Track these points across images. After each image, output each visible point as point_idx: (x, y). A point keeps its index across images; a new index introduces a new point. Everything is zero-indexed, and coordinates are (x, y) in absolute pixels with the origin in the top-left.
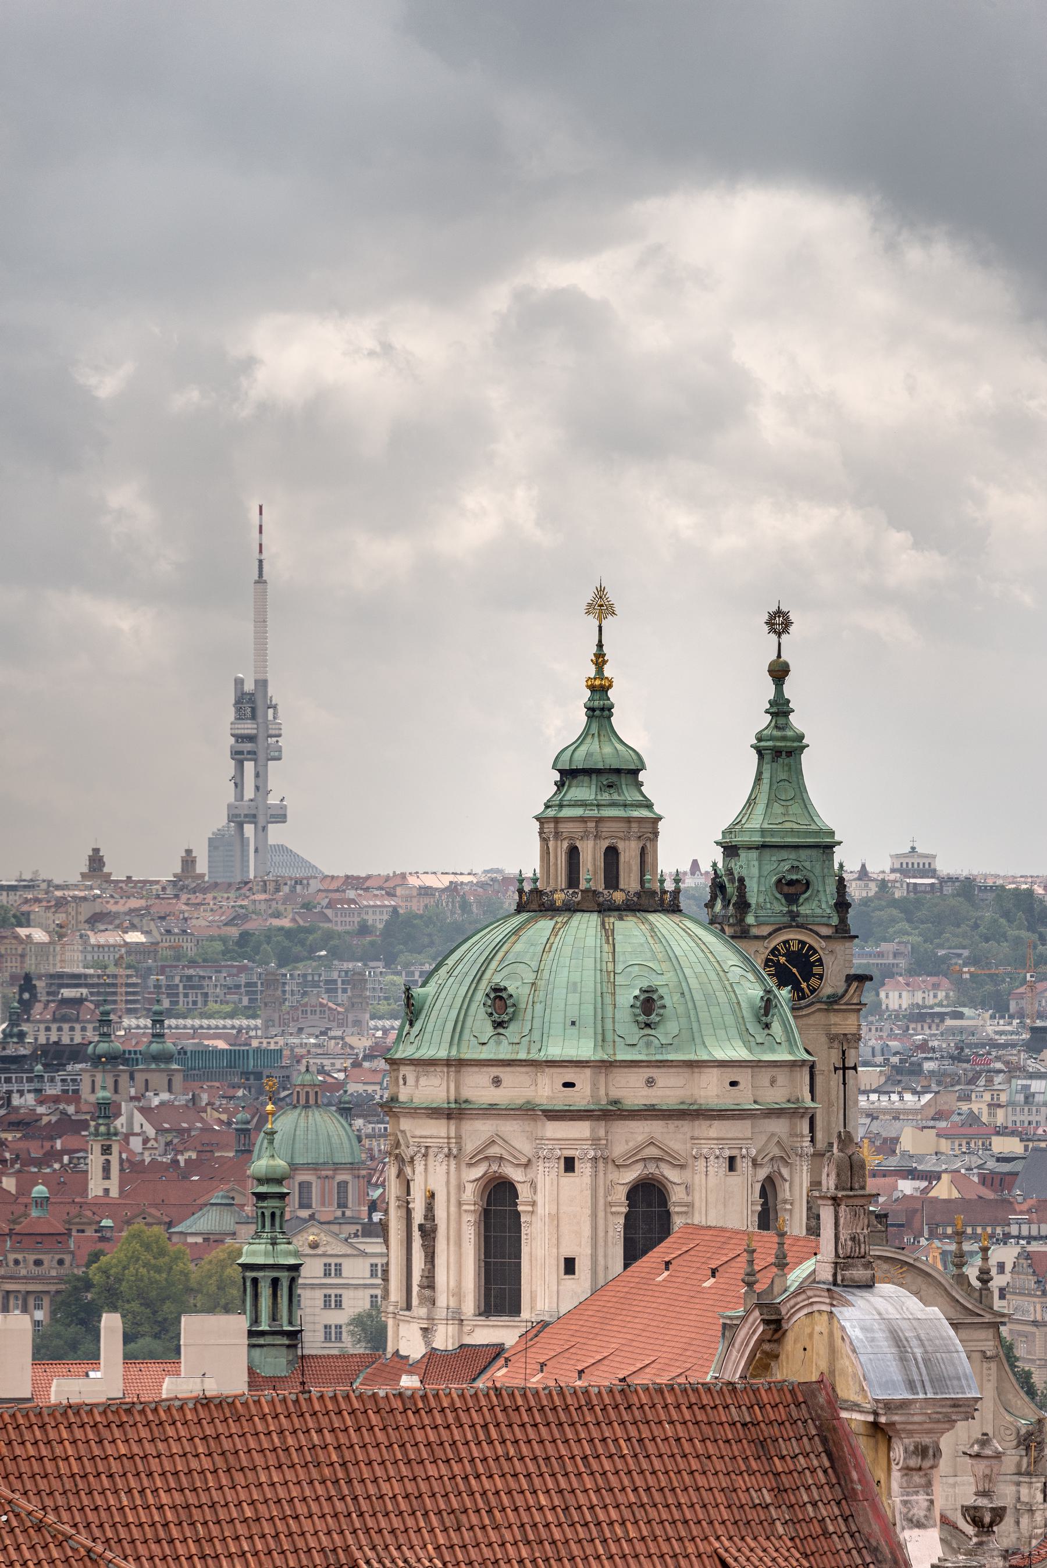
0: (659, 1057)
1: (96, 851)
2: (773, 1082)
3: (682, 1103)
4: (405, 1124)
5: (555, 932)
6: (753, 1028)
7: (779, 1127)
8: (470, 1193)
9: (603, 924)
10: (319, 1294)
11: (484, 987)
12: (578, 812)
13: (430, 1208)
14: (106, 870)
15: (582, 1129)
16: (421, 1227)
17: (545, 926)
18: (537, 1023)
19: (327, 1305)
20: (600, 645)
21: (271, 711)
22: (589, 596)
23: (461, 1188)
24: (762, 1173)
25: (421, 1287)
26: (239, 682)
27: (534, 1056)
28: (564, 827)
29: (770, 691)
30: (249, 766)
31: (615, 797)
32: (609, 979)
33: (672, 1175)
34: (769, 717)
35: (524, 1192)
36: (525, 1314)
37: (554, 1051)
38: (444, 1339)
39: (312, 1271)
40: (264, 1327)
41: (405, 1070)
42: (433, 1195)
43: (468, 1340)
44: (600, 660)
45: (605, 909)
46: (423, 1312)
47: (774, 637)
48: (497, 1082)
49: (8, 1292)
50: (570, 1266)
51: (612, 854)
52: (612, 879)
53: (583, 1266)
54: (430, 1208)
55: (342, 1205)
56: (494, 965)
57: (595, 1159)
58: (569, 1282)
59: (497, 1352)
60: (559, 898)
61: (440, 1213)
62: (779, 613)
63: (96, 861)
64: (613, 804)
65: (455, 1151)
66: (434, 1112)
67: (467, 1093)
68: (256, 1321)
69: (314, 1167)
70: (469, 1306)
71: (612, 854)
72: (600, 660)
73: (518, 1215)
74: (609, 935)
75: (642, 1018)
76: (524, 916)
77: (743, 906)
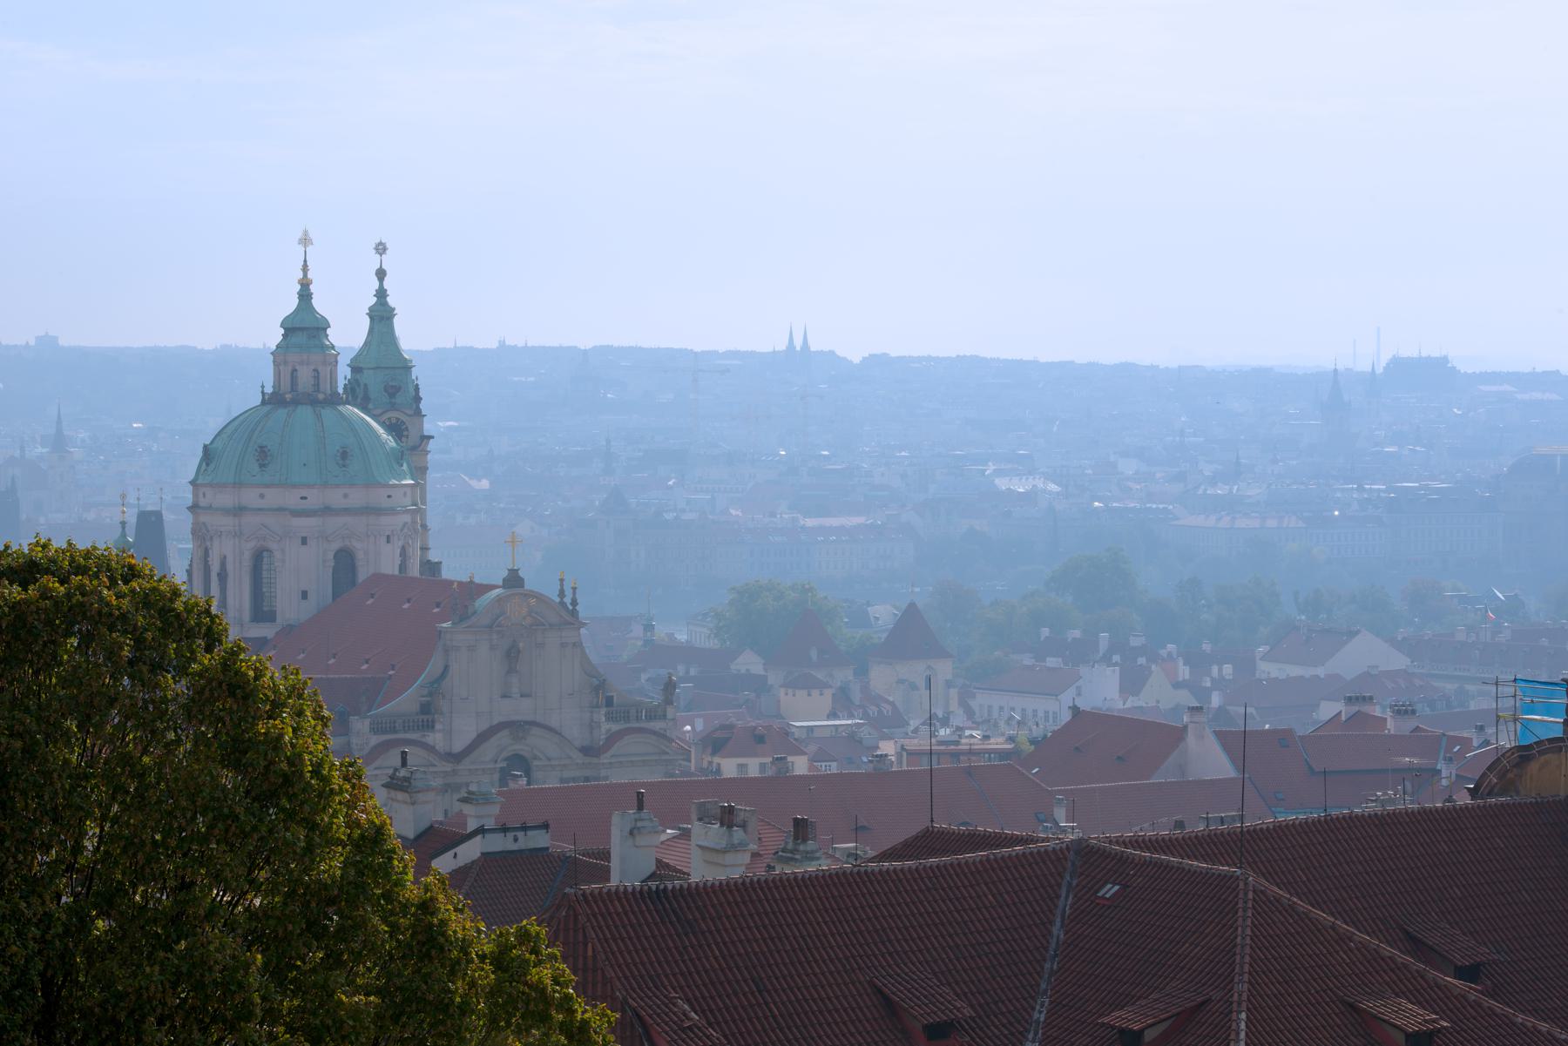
17: (282, 413)
20: (305, 261)
22: (300, 235)
29: (376, 285)
34: (376, 299)
36: (279, 620)
42: (225, 557)
44: (305, 268)
45: (314, 402)
47: (379, 256)
48: (262, 496)
50: (304, 595)
61: (230, 567)
62: (381, 243)
66: (226, 511)
70: (247, 616)
72: (305, 268)
74: (319, 417)
75: (341, 462)
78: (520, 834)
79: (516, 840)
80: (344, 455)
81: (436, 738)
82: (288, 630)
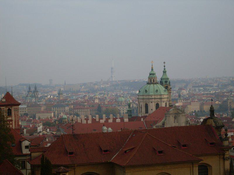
4: (139, 100)
7: (166, 99)
8: (144, 105)
11: (145, 90)
13: (141, 106)
17: (149, 85)
32: (154, 89)
33: (159, 103)
35: (148, 104)
37: (150, 94)
38: (143, 115)
39: (122, 108)
45: (153, 84)
50: (152, 110)
51: (154, 80)
52: (154, 81)
54: (141, 106)
59: (146, 116)
63: (102, 80)
66: (142, 99)
70: (145, 113)
71: (154, 80)
72: (152, 66)
77: (163, 83)
80: (157, 91)
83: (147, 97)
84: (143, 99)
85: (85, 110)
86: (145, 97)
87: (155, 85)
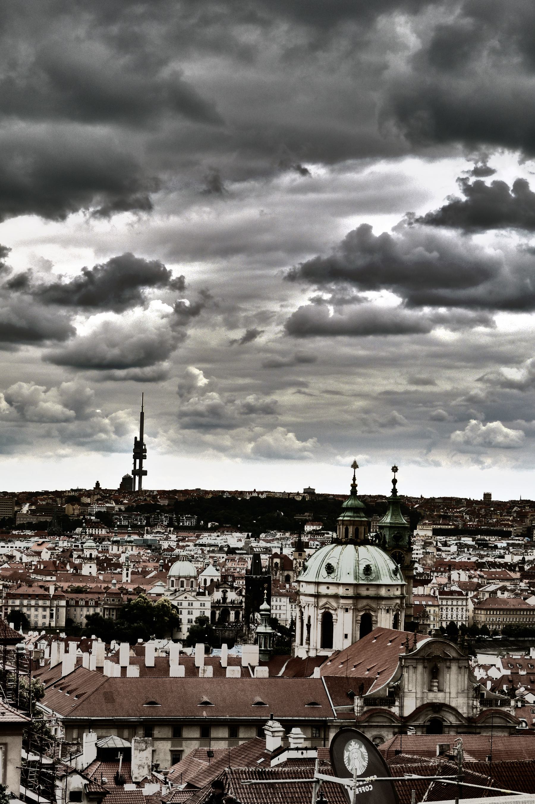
0: (370, 583)
1: (98, 482)
2: (397, 590)
3: (376, 595)
4: (302, 597)
5: (343, 549)
6: (393, 576)
8: (320, 617)
9: (355, 548)
10: (187, 610)
12: (348, 518)
14: (100, 487)
15: (350, 601)
16: (307, 625)
17: (340, 548)
18: (339, 573)
19: (189, 613)
20: (354, 476)
21: (144, 446)
22: (352, 463)
23: (317, 615)
24: (394, 613)
25: (306, 640)
26: (136, 438)
27: (338, 582)
28: (345, 523)
29: (392, 487)
30: (138, 461)
31: (358, 515)
32: (358, 563)
34: (392, 493)
35: (334, 617)
38: (312, 654)
39: (185, 604)
40: (263, 648)
41: (301, 584)
43: (318, 654)
44: (354, 479)
46: (307, 646)
47: (393, 473)
48: (328, 588)
49: (105, 608)
50: (346, 636)
53: (350, 637)
55: (192, 587)
56: (327, 557)
57: (353, 609)
58: (346, 640)
59: (326, 658)
60: (344, 540)
62: (395, 467)
63: (98, 484)
64: (357, 517)
65: (316, 605)
67: (320, 591)
68: (260, 647)
69: (185, 577)
72: (354, 479)
73: (333, 622)
74: (357, 551)
76: (334, 545)
78: (304, 752)
79: (302, 753)
81: (395, 710)
82: (338, 652)
83: (333, 590)
84: (317, 596)
85: (48, 603)
86: (323, 590)
87: (361, 549)
